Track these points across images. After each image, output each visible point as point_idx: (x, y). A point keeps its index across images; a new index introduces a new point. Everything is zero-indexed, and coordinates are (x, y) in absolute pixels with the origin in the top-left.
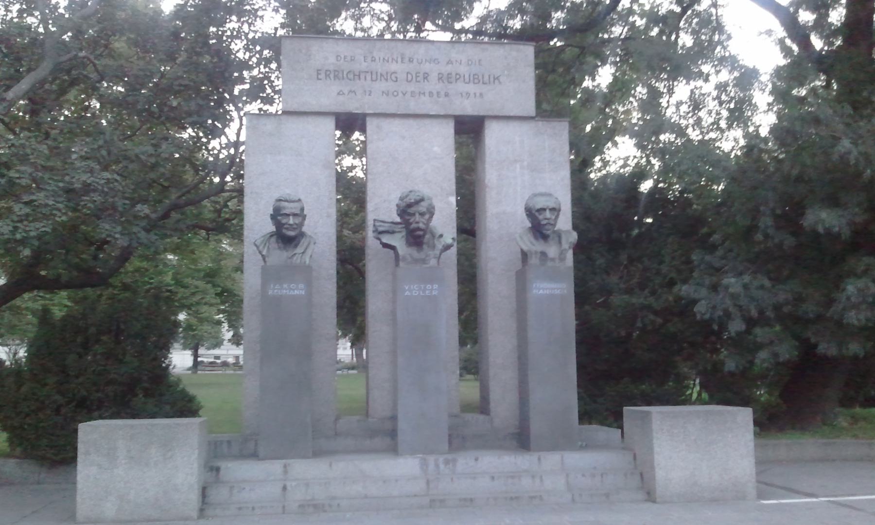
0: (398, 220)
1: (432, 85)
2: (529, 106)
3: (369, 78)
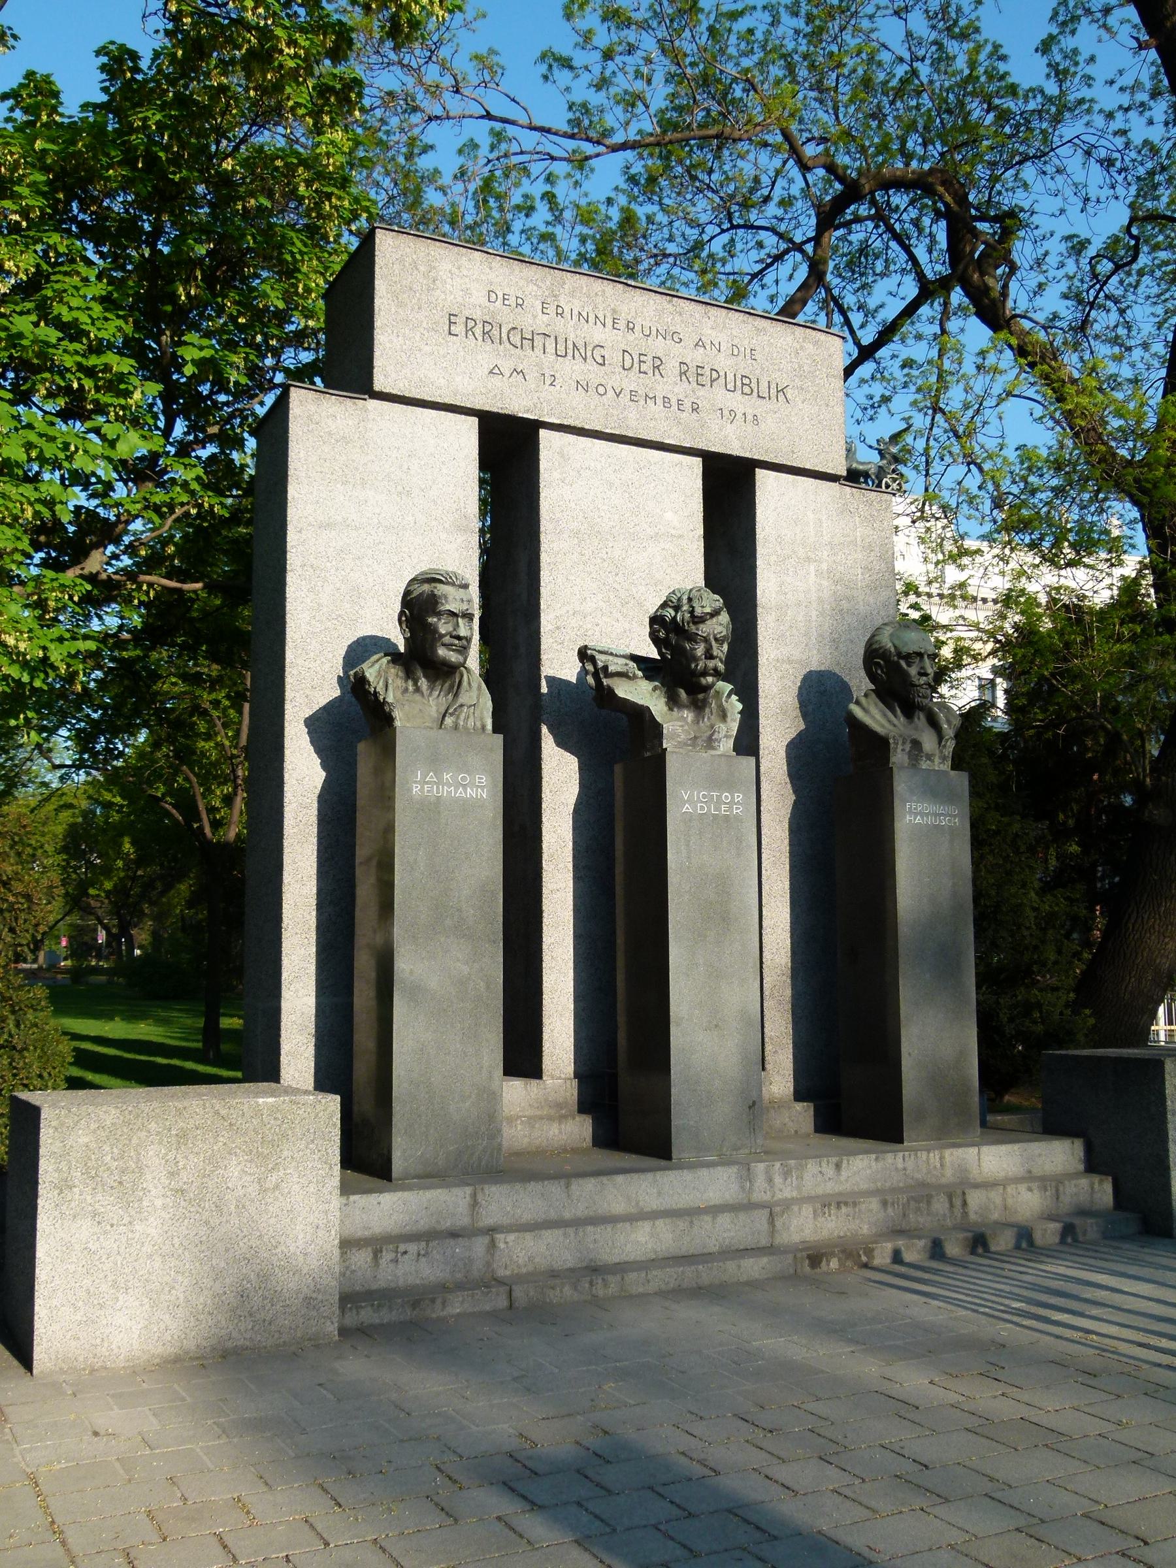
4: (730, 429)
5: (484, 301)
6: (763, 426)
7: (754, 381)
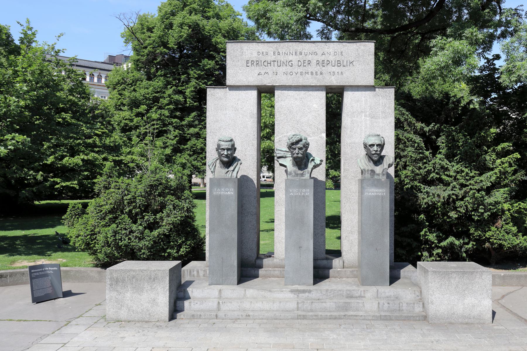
0: (288, 150)
1: (314, 68)
2: (370, 80)
3: (276, 65)
4: (333, 77)
5: (256, 55)
6: (344, 75)
7: (342, 62)
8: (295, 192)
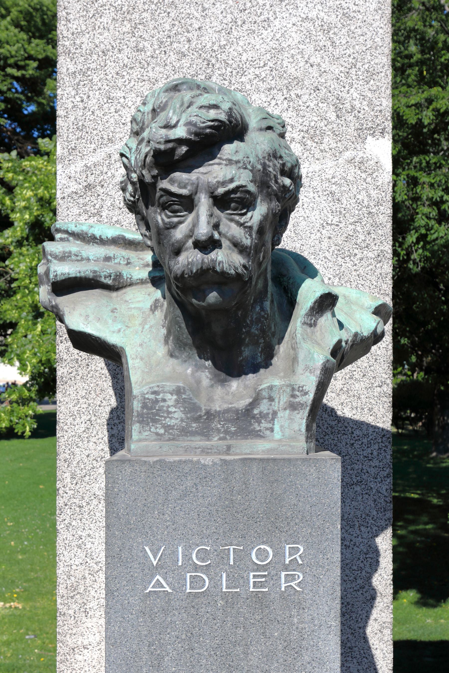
0: (128, 226)
8: (184, 565)
